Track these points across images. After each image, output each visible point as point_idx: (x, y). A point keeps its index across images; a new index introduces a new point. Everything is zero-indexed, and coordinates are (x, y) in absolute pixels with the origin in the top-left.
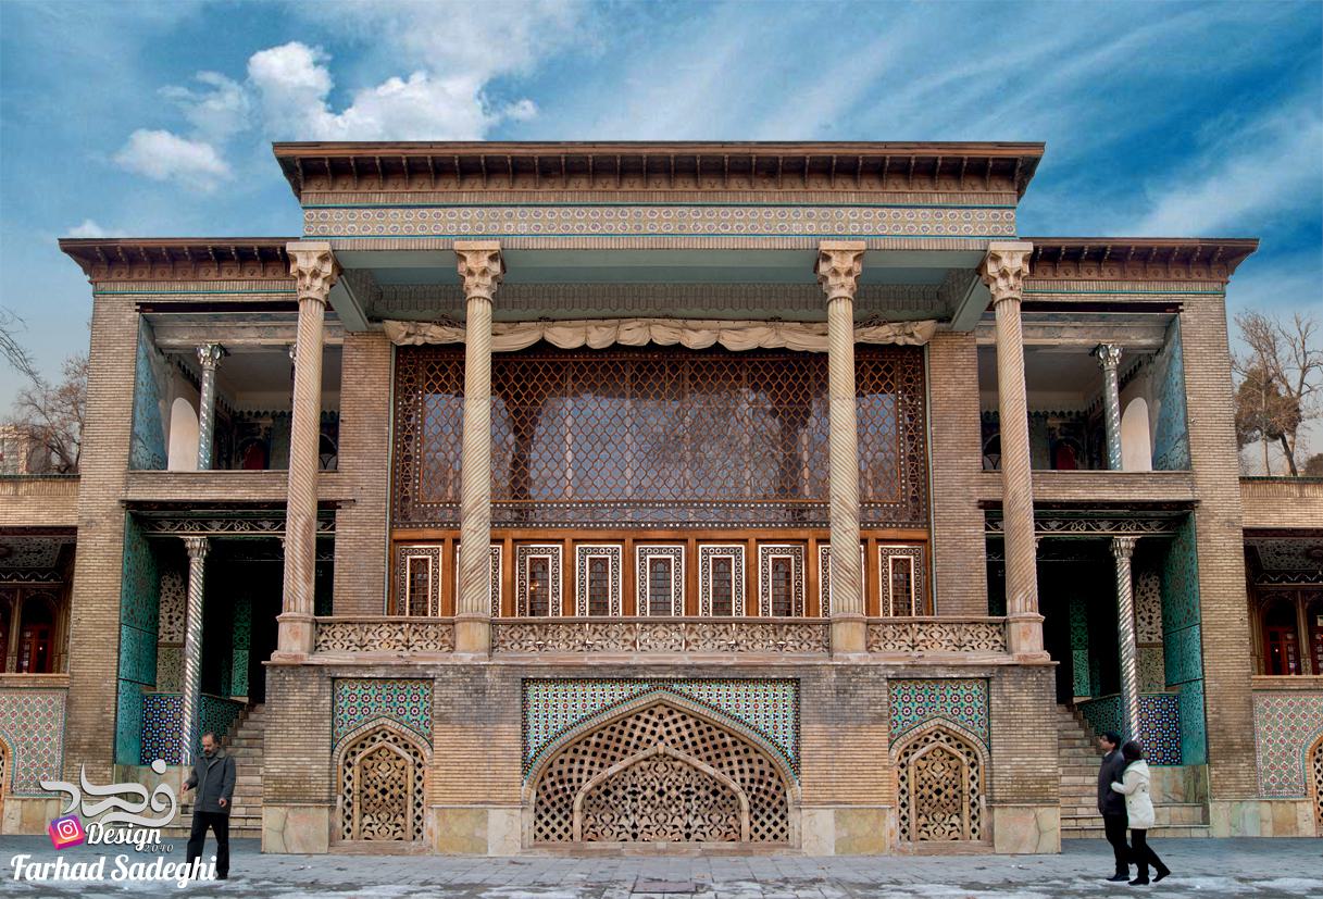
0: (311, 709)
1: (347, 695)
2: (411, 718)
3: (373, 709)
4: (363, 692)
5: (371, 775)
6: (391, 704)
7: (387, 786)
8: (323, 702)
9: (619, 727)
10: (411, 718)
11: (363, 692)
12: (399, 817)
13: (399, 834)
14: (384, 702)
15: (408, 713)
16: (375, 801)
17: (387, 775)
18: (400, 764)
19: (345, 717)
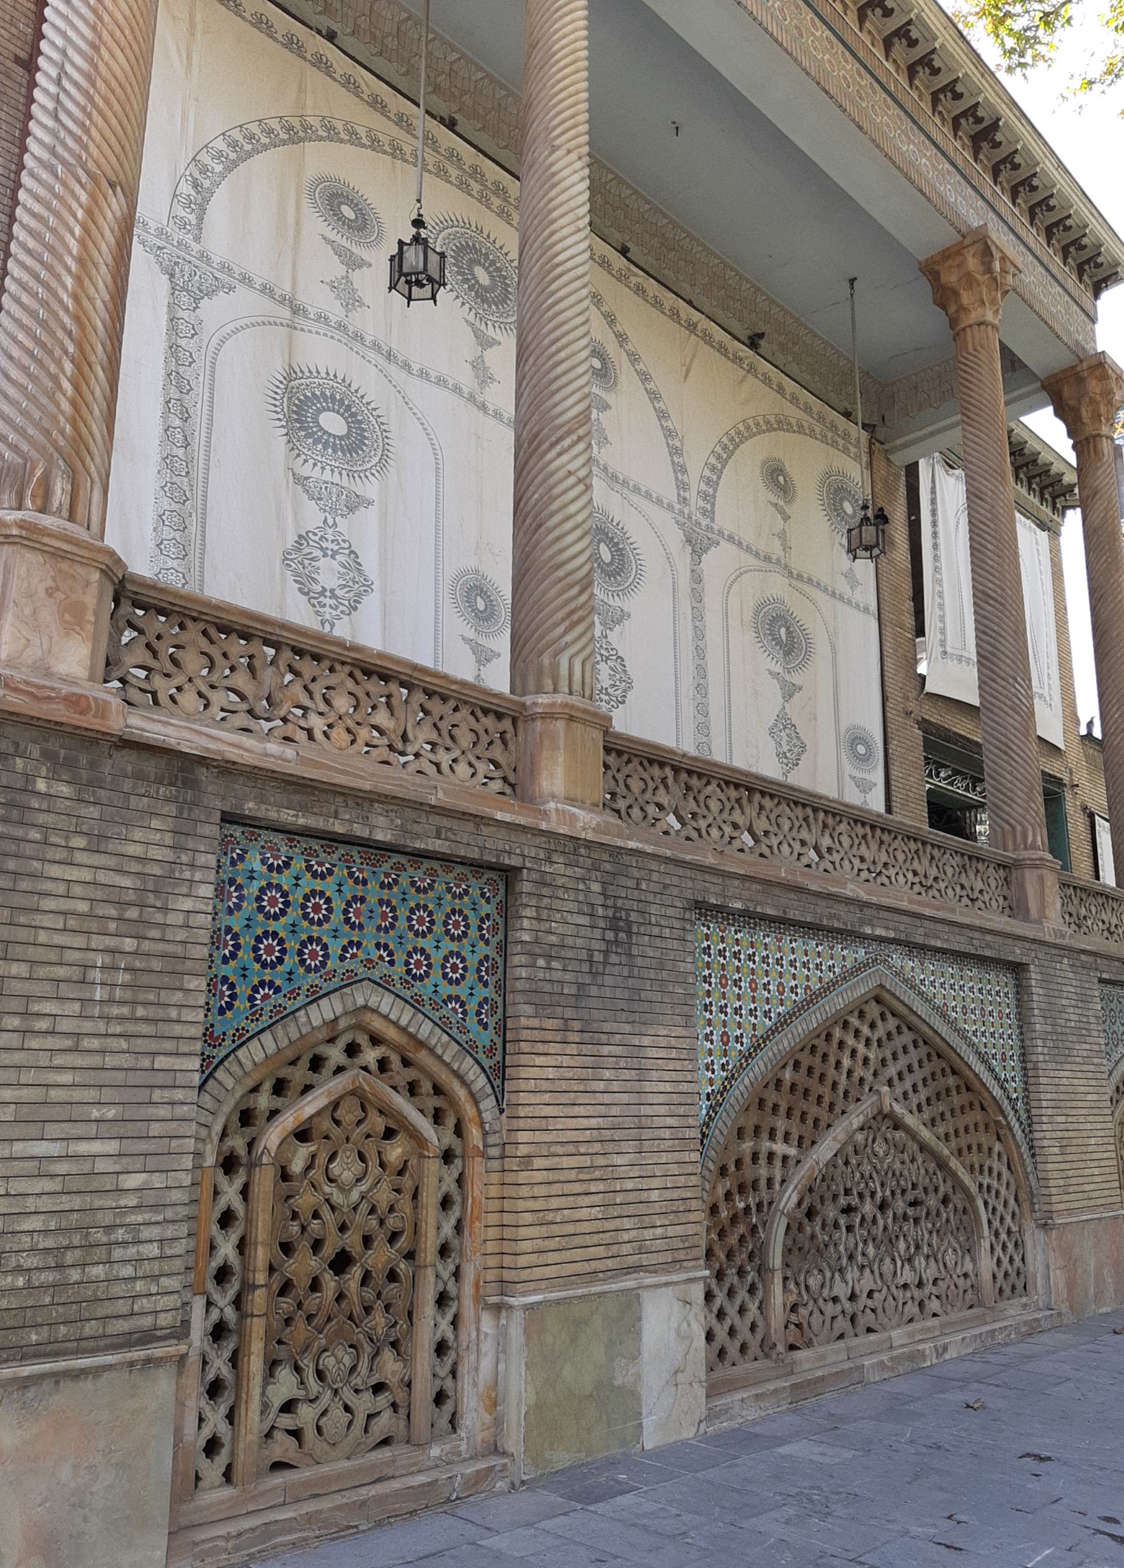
0: (138, 929)
1: (253, 888)
2: (446, 990)
3: (335, 948)
4: (308, 883)
5: (306, 1200)
6: (390, 939)
7: (352, 1241)
8: (188, 904)
9: (820, 1043)
10: (446, 990)
11: (308, 883)
12: (388, 1354)
13: (385, 1423)
14: (370, 929)
15: (436, 975)
16: (312, 1302)
17: (355, 1196)
18: (395, 1152)
19: (244, 972)
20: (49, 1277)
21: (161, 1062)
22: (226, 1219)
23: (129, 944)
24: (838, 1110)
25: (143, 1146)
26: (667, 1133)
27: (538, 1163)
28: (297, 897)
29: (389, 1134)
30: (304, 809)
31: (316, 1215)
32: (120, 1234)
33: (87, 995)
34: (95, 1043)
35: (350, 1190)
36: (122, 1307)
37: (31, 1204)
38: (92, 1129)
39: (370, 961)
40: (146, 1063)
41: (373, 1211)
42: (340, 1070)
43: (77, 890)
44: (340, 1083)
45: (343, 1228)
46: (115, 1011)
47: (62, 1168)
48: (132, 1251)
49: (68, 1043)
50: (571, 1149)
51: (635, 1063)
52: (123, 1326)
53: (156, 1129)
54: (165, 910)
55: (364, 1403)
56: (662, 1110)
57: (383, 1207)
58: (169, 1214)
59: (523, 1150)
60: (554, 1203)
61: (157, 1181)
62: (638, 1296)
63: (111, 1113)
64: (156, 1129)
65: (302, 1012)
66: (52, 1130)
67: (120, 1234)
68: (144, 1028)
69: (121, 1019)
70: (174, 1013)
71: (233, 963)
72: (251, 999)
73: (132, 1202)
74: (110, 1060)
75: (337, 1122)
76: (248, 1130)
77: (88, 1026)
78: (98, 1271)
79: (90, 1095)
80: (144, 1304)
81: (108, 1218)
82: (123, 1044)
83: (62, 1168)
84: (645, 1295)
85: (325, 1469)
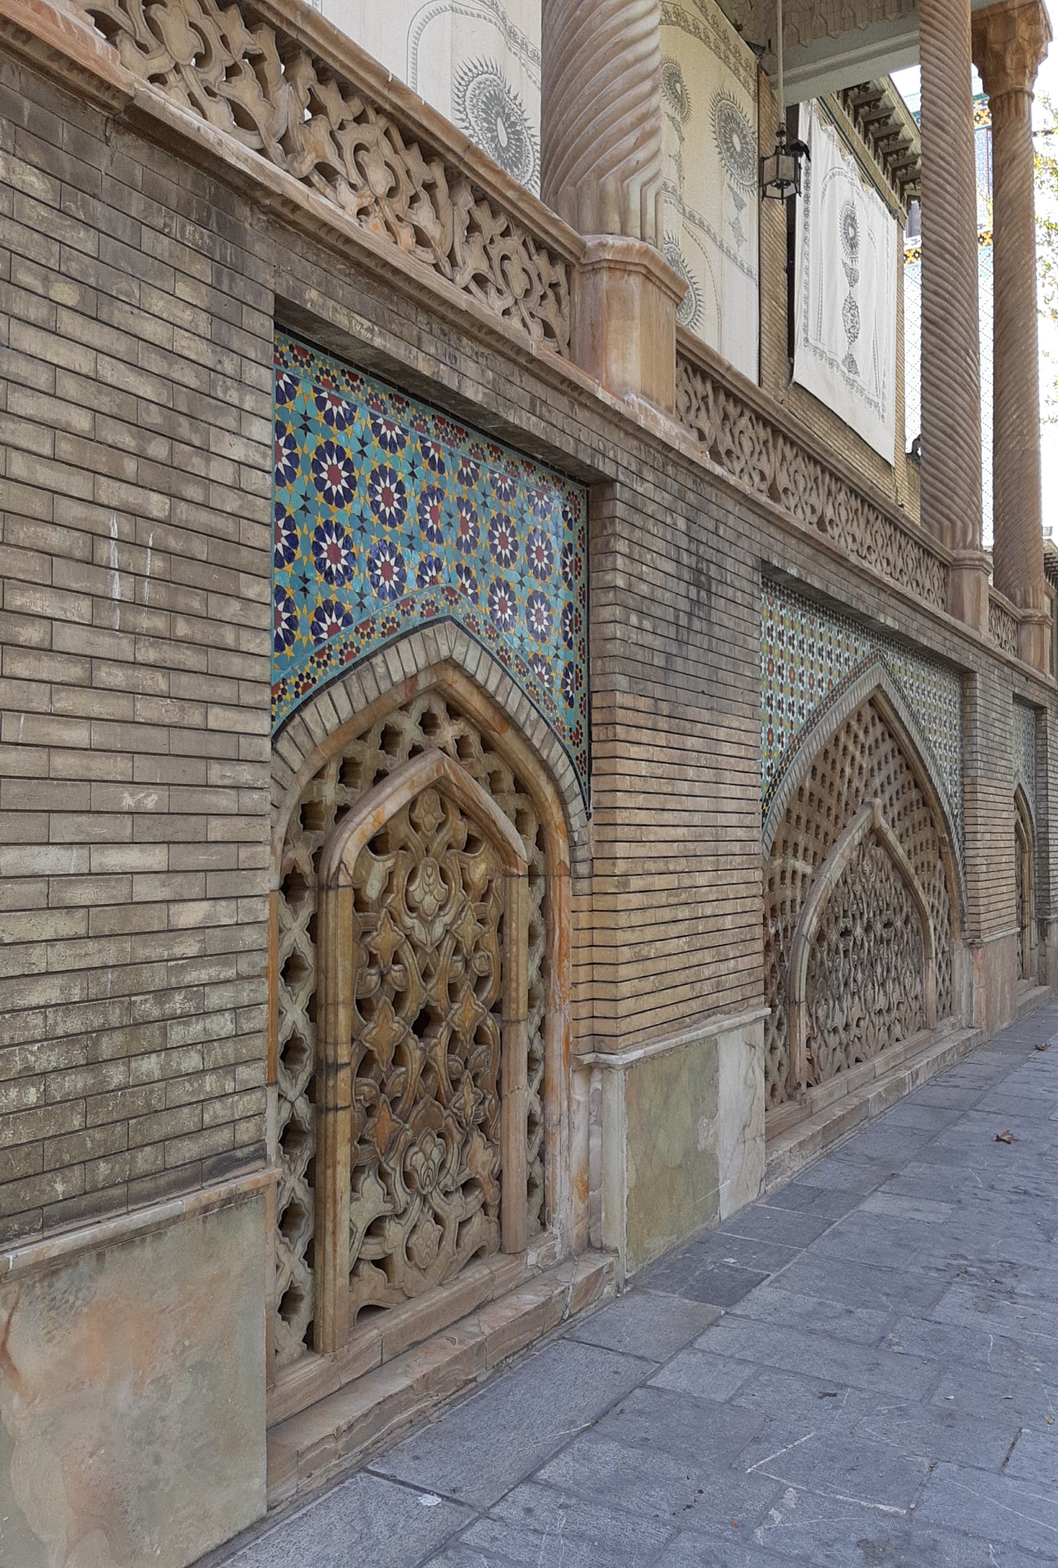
5: (384, 938)
12: (477, 1141)
14: (450, 540)
17: (438, 930)
18: (479, 869)
20: (76, 1083)
21: (218, 718)
22: (291, 969)
23: (157, 505)
24: (841, 824)
25: (200, 858)
26: (736, 848)
27: (636, 883)
28: (363, 472)
29: (471, 844)
30: (380, 322)
31: (396, 960)
32: (178, 1003)
33: (99, 589)
34: (117, 677)
35: (433, 922)
36: (187, 1119)
37: (39, 958)
38: (125, 828)
39: (452, 591)
40: (195, 717)
41: (457, 951)
42: (415, 751)
43: (70, 387)
44: (422, 770)
45: (426, 975)
46: (146, 622)
47: (83, 894)
48: (196, 1029)
49: (75, 672)
50: (661, 865)
51: (712, 760)
52: (189, 1150)
53: (217, 829)
54: (205, 451)
55: (454, 1208)
56: (734, 819)
57: (468, 945)
58: (244, 966)
59: (621, 867)
60: (649, 933)
61: (225, 913)
62: (716, 1042)
63: (151, 800)
64: (217, 829)
65: (378, 660)
66: (64, 828)
67: (178, 1003)
68: (190, 659)
69: (157, 638)
70: (229, 637)
71: (289, 567)
72: (316, 630)
73: (190, 947)
74: (145, 710)
75: (415, 826)
76: (312, 835)
77: (105, 645)
78: (150, 1065)
79: (118, 767)
80: (218, 1110)
81: (158, 977)
82: (160, 682)
83: (83, 894)
84: (721, 1040)
85: (422, 1306)
